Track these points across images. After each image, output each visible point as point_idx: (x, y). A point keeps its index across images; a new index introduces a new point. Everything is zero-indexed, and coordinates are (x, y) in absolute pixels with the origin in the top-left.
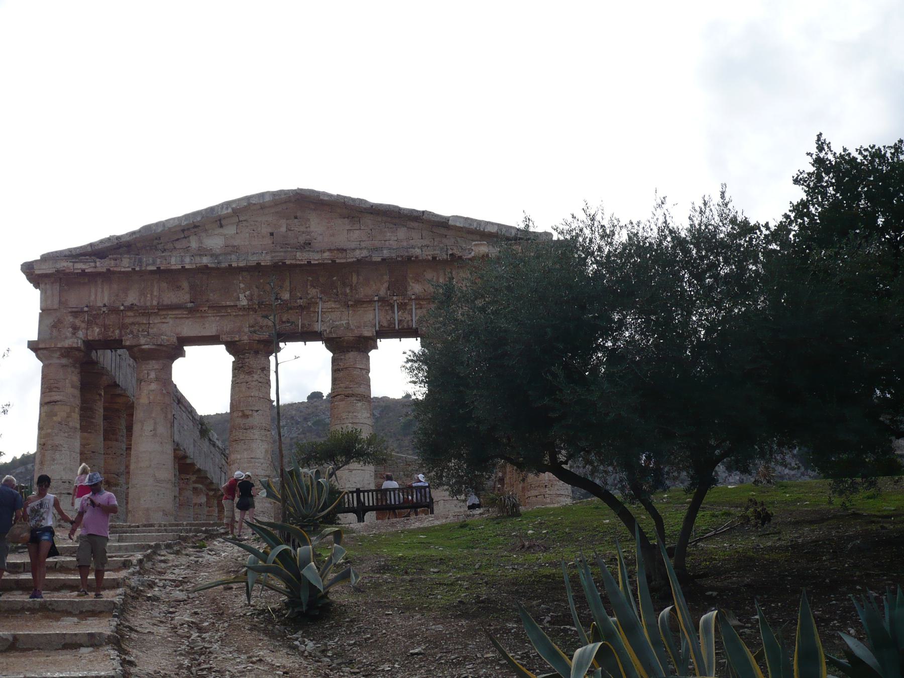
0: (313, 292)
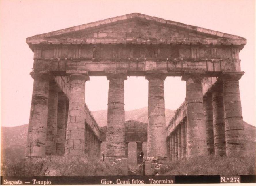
0: (142, 56)
